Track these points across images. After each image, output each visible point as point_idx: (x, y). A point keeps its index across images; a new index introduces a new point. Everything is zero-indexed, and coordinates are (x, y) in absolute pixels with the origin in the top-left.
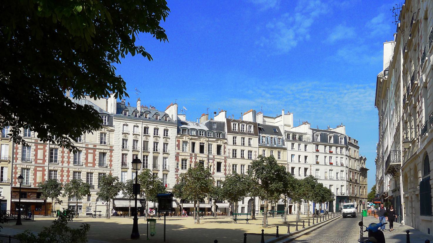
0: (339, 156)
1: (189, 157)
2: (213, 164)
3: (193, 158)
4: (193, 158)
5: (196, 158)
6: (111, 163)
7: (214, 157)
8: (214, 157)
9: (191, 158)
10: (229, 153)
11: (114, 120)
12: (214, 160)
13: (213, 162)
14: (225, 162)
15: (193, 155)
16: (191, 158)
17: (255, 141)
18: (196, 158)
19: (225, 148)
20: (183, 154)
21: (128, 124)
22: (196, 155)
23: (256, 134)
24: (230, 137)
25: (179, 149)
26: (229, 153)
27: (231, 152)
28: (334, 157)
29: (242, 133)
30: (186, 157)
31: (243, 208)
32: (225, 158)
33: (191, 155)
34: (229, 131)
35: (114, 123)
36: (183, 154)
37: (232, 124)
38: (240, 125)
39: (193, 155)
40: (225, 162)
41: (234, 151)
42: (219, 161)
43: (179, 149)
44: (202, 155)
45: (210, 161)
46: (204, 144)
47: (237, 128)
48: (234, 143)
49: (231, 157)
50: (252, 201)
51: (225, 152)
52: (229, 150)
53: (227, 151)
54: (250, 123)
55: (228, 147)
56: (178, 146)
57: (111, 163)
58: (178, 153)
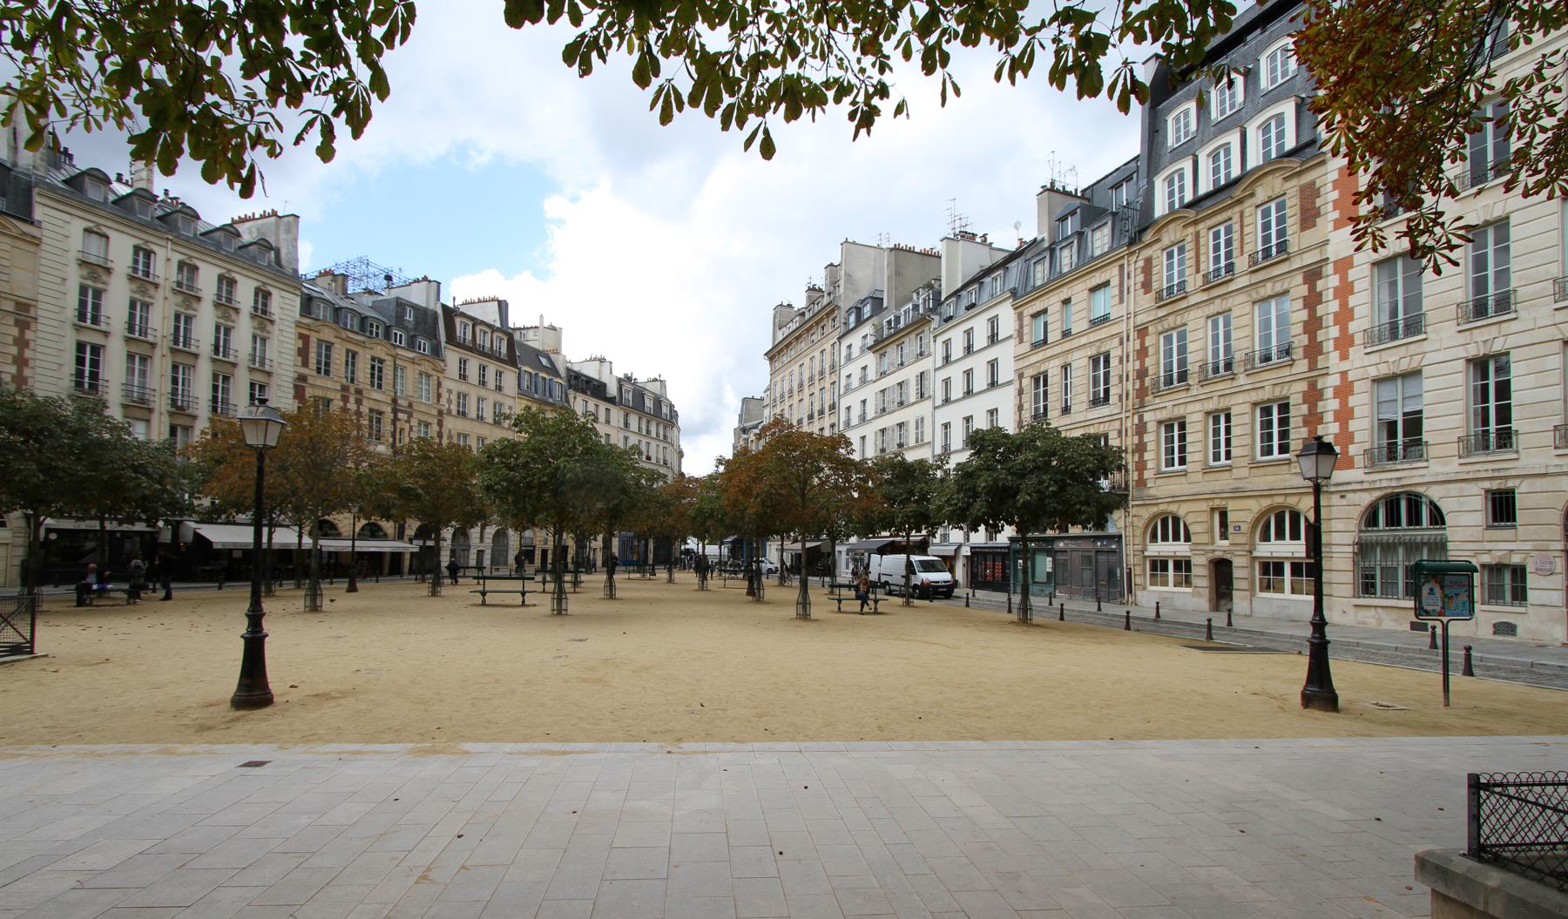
0: (662, 445)
1: (339, 396)
2: (407, 426)
3: (352, 399)
4: (352, 399)
5: (359, 402)
6: (20, 371)
7: (410, 405)
8: (410, 405)
9: (345, 399)
10: (450, 401)
11: (37, 198)
12: (410, 415)
13: (408, 421)
14: (440, 424)
15: (352, 390)
16: (345, 399)
17: (510, 377)
18: (359, 402)
19: (439, 385)
20: (319, 382)
21: (105, 230)
22: (359, 392)
23: (512, 360)
24: (452, 356)
25: (305, 364)
26: (450, 401)
27: (454, 397)
28: (653, 444)
29: (482, 353)
30: (330, 395)
31: (480, 553)
32: (440, 413)
33: (345, 388)
34: (451, 338)
35: (39, 213)
36: (319, 382)
37: (458, 321)
38: (478, 328)
39: (352, 390)
40: (440, 424)
41: (463, 396)
42: (424, 418)
43: (305, 364)
44: (376, 395)
45: (400, 415)
46: (381, 361)
47: (469, 337)
48: (463, 377)
49: (454, 412)
50: (500, 536)
51: (439, 396)
52: (450, 391)
53: (445, 396)
54: (498, 330)
55: (447, 384)
56: (303, 353)
57: (20, 371)
58: (302, 378)
